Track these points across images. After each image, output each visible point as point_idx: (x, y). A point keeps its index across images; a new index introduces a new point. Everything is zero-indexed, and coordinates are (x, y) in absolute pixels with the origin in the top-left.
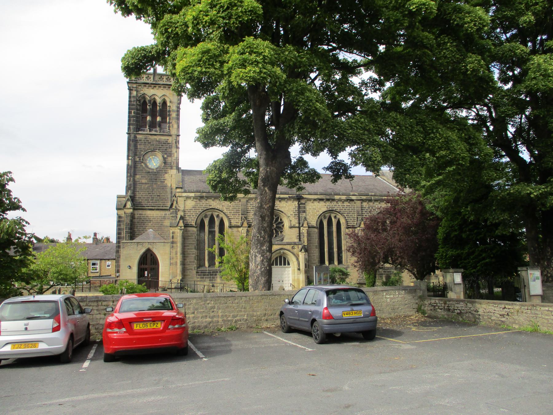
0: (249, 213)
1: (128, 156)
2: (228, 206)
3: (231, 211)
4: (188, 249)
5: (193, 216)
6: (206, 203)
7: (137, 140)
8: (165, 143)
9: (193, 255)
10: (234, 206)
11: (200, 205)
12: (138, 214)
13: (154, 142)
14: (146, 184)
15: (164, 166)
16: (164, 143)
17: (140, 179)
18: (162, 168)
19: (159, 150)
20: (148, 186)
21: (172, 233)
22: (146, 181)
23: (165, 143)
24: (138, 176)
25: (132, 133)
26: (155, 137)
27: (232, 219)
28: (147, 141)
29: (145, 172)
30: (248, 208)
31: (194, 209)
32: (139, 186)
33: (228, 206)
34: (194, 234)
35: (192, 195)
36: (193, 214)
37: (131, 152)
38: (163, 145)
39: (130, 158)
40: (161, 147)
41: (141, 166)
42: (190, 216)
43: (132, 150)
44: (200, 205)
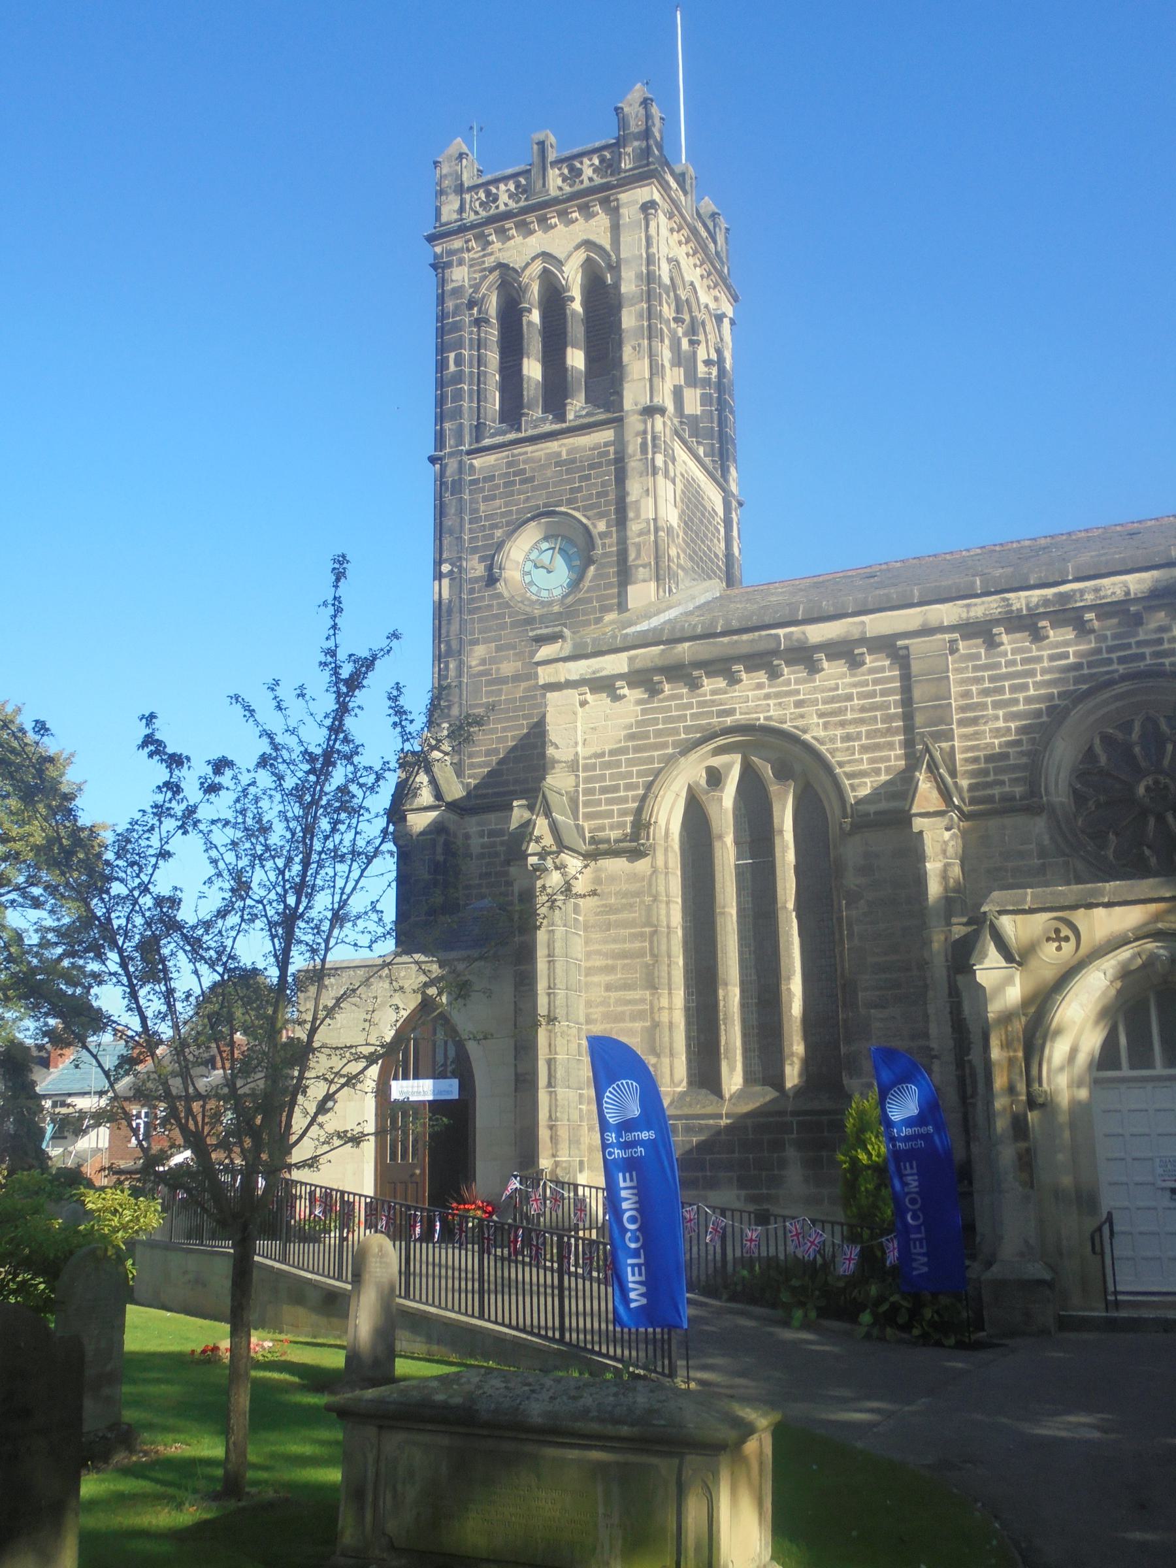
0: (974, 721)
1: (438, 563)
2: (833, 700)
3: (851, 730)
4: (608, 988)
5: (629, 787)
6: (701, 704)
7: (474, 482)
8: (600, 465)
9: (638, 1025)
10: (873, 694)
11: (667, 720)
12: (481, 834)
13: (549, 473)
14: (517, 678)
15: (595, 577)
16: (592, 467)
17: (493, 661)
18: (587, 592)
19: (570, 502)
20: (526, 690)
21: (521, 900)
22: (519, 664)
23: (600, 465)
24: (480, 651)
25: (451, 455)
26: (553, 446)
27: (862, 774)
28: (515, 474)
29: (514, 625)
30: (967, 694)
31: (637, 749)
32: (489, 693)
33: (833, 700)
34: (638, 894)
35: (616, 664)
36: (630, 775)
37: (445, 542)
38: (588, 478)
39: (445, 568)
40: (580, 489)
41: (492, 597)
42: (616, 789)
43: (451, 535)
44: (667, 720)
